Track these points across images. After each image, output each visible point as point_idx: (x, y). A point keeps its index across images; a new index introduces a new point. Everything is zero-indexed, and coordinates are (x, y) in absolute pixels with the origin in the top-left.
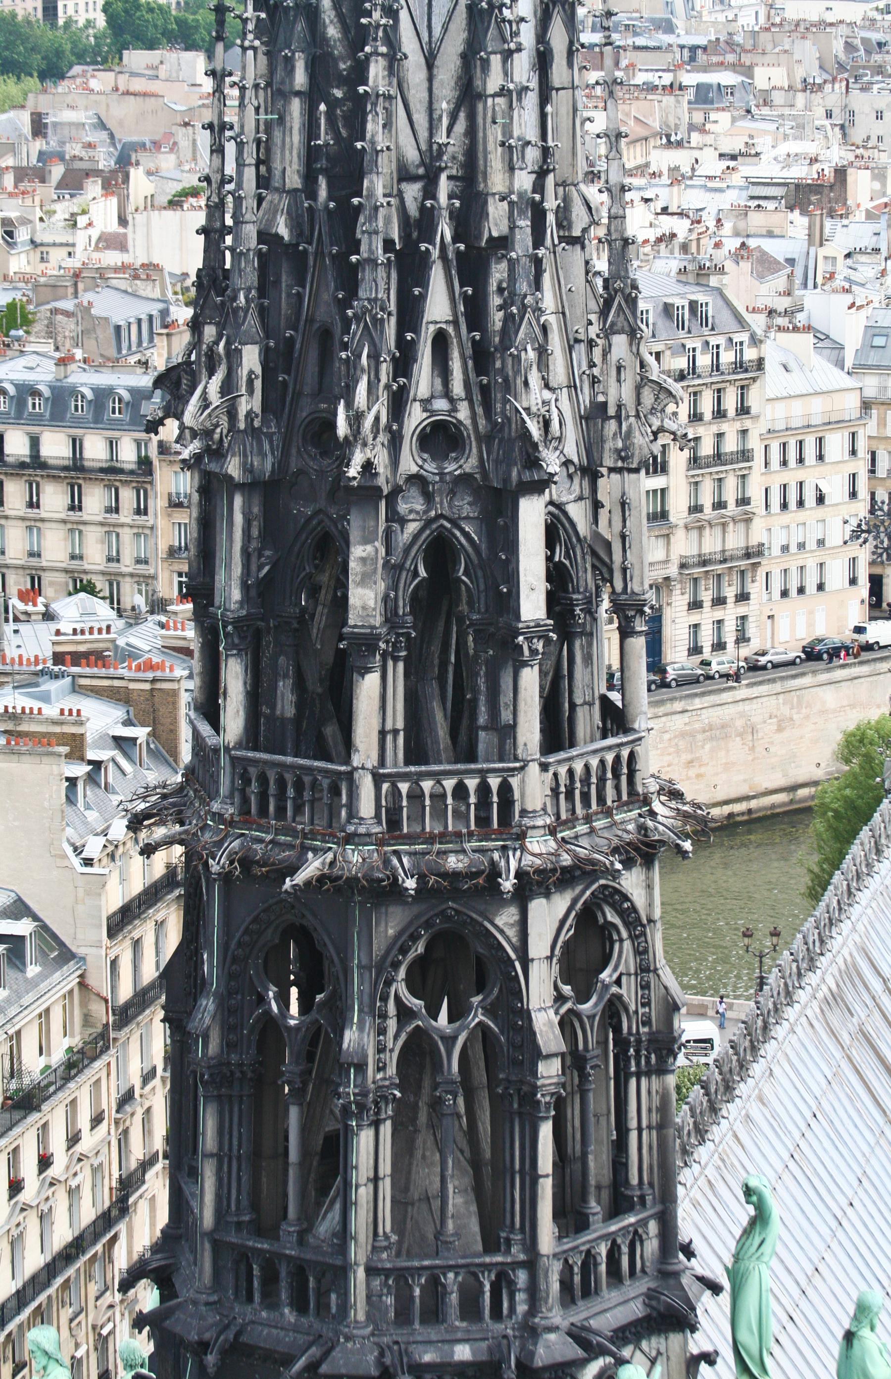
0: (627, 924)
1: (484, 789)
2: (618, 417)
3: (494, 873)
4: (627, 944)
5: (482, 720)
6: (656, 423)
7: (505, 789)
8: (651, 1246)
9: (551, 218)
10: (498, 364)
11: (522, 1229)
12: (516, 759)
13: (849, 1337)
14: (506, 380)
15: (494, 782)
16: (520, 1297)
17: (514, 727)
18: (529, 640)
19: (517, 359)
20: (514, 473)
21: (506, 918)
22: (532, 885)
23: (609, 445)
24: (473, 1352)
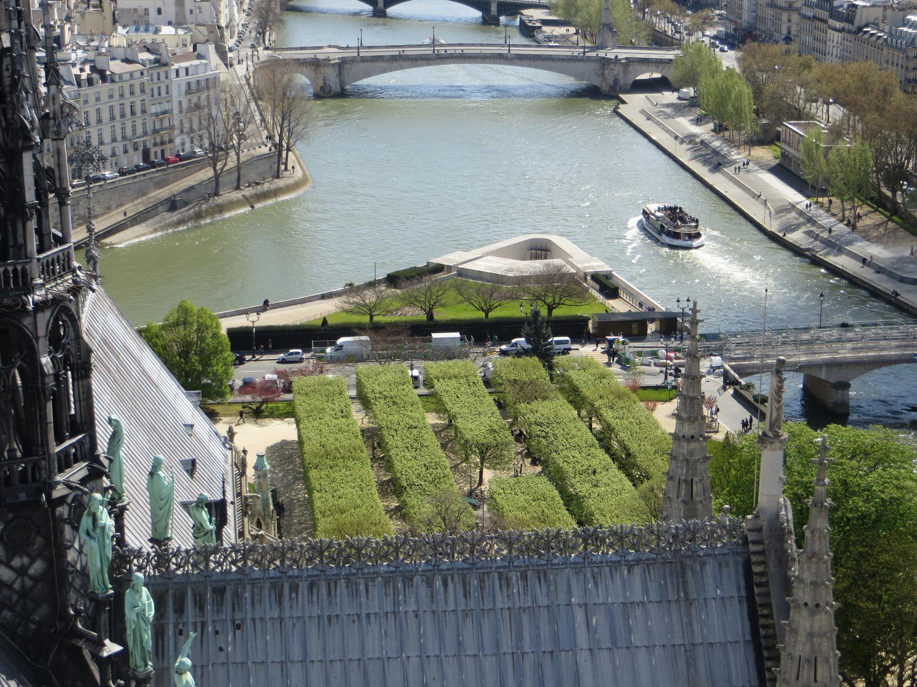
0: (70, 320)
1: (15, 271)
2: (54, 118)
3: (25, 304)
4: (71, 328)
5: (11, 243)
6: (70, 120)
7: (24, 270)
8: (87, 446)
9: (24, 39)
10: (9, 99)
11: (42, 445)
12: (27, 258)
13: (152, 474)
14: (14, 104)
15: (19, 268)
16: (43, 471)
17: (25, 244)
18: (30, 210)
19: (18, 97)
20: (20, 142)
21: (27, 321)
22: (39, 307)
23: (51, 129)
24: (28, 496)
